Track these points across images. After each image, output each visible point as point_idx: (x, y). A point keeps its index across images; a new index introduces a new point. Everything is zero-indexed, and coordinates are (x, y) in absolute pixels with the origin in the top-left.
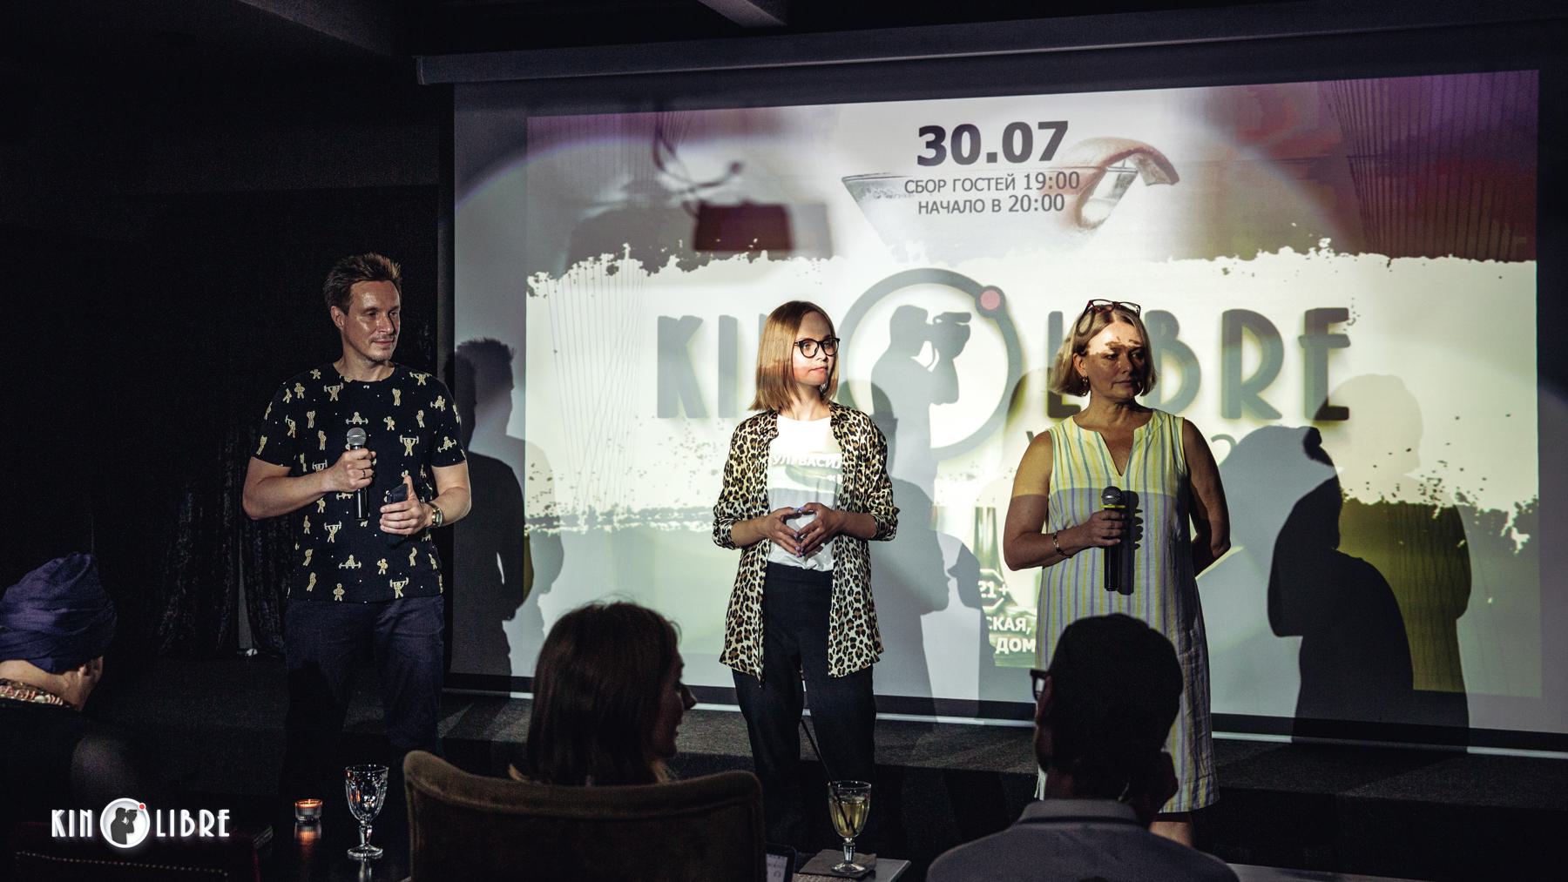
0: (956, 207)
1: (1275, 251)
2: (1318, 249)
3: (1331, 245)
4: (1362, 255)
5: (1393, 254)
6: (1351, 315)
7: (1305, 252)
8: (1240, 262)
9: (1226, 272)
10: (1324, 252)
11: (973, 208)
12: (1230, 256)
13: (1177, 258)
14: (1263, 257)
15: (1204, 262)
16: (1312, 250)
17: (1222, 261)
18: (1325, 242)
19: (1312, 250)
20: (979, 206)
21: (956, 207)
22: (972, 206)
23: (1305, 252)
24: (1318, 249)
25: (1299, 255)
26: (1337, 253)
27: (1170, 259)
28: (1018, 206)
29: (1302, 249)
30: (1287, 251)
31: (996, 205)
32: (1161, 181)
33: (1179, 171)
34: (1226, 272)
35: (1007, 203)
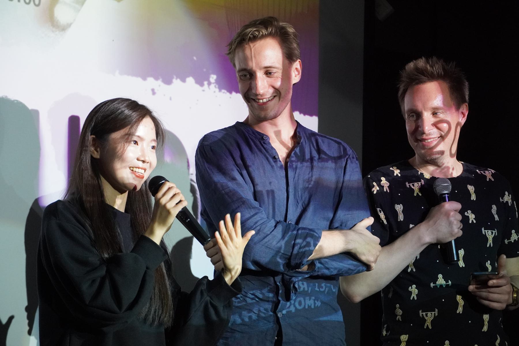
1: (184, 81)
2: (209, 84)
3: (217, 81)
4: (234, 93)
7: (202, 85)
9: (154, 92)
10: (212, 86)
12: (156, 79)
14: (177, 82)
15: (139, 79)
16: (206, 83)
18: (213, 78)
19: (206, 83)
23: (202, 85)
24: (209, 84)
25: (198, 86)
26: (220, 89)
29: (200, 82)
30: (190, 80)
34: (154, 92)
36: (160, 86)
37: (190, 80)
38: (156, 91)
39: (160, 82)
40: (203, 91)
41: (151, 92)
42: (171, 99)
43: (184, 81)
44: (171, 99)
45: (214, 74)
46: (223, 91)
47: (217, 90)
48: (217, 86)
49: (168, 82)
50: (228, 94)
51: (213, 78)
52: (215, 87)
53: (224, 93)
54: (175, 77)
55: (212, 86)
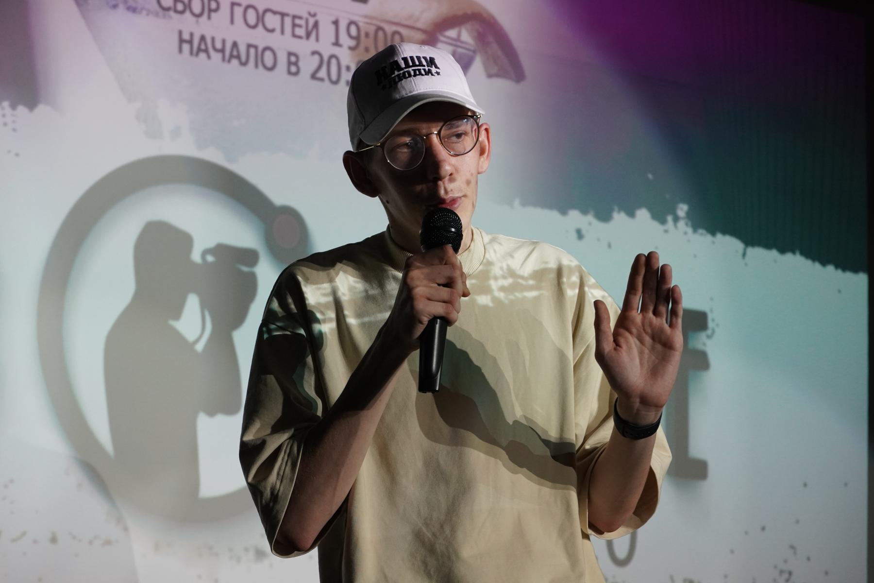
0: (232, 53)
1: (631, 214)
2: (676, 219)
3: (689, 215)
4: (719, 236)
5: (750, 241)
6: (710, 324)
7: (663, 221)
8: (596, 223)
10: (681, 224)
11: (259, 61)
12: (584, 212)
13: (524, 204)
14: (619, 218)
15: (554, 215)
16: (670, 218)
17: (575, 218)
18: (682, 209)
19: (670, 218)
20: (268, 57)
21: (232, 53)
22: (259, 57)
24: (676, 219)
25: (656, 225)
26: (695, 228)
27: (517, 202)
28: (323, 73)
29: (659, 217)
30: (643, 214)
31: (293, 62)
32: (501, 74)
33: (526, 62)
34: (580, 235)
35: (308, 65)
36: (590, 224)
37: (643, 214)
38: (584, 232)
39: (590, 218)
40: (666, 231)
41: (574, 235)
42: (609, 246)
43: (631, 214)
44: (609, 246)
45: (683, 202)
46: (701, 231)
47: (690, 230)
48: (690, 223)
49: (604, 216)
50: (709, 237)
51: (682, 209)
52: (687, 224)
53: (702, 234)
54: (616, 208)
55: (681, 224)
